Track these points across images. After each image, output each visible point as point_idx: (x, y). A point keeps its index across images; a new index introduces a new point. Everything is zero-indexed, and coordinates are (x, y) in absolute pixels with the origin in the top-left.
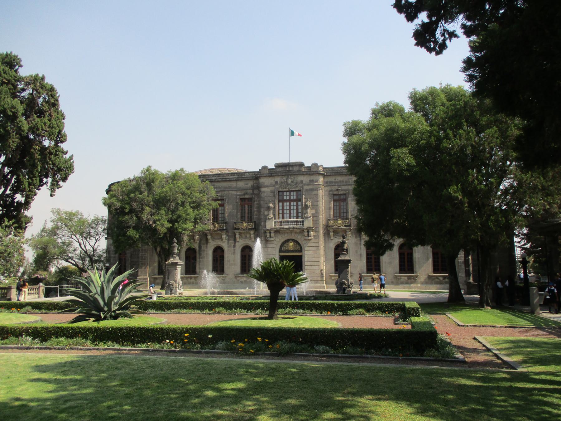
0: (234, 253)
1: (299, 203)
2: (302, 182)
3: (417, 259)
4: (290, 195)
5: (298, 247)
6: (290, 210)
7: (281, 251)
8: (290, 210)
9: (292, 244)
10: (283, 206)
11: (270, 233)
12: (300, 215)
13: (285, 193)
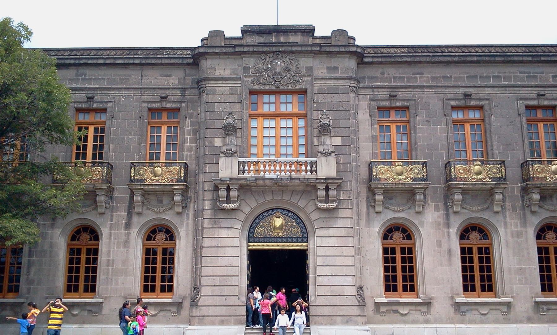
0: (126, 243)
5: (296, 230)
7: (251, 239)
9: (278, 222)
11: (228, 190)
13: (266, 98)
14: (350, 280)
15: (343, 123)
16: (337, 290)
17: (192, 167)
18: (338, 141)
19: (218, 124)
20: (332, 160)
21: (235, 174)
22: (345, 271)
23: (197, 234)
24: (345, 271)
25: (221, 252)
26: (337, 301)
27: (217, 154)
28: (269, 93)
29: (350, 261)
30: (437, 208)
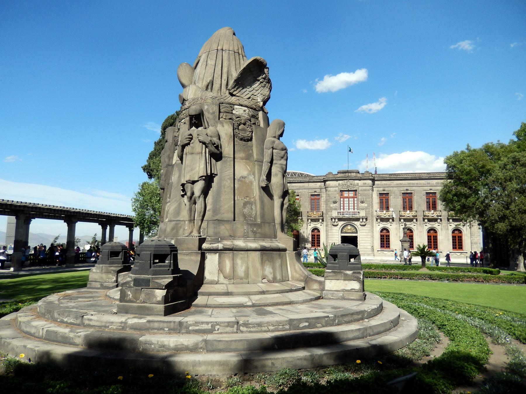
1: (356, 199)
2: (358, 184)
3: (441, 241)
4: (349, 194)
6: (349, 204)
7: (342, 232)
8: (349, 204)
10: (344, 201)
12: (356, 207)
14: (369, 244)
15: (368, 200)
16: (366, 247)
17: (324, 212)
18: (366, 205)
19: (331, 200)
20: (364, 211)
21: (337, 215)
22: (368, 242)
23: (327, 231)
24: (368, 242)
25: (333, 236)
26: (365, 250)
27: (332, 209)
28: (346, 191)
29: (369, 239)
30: (396, 224)
